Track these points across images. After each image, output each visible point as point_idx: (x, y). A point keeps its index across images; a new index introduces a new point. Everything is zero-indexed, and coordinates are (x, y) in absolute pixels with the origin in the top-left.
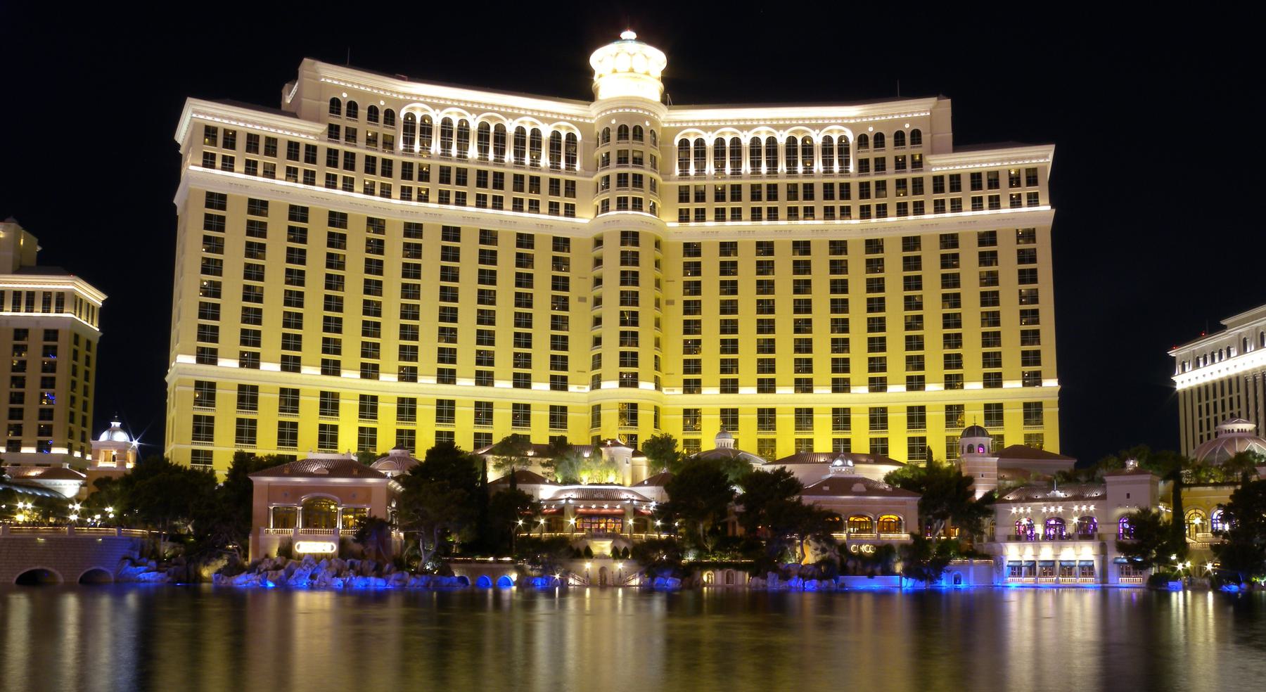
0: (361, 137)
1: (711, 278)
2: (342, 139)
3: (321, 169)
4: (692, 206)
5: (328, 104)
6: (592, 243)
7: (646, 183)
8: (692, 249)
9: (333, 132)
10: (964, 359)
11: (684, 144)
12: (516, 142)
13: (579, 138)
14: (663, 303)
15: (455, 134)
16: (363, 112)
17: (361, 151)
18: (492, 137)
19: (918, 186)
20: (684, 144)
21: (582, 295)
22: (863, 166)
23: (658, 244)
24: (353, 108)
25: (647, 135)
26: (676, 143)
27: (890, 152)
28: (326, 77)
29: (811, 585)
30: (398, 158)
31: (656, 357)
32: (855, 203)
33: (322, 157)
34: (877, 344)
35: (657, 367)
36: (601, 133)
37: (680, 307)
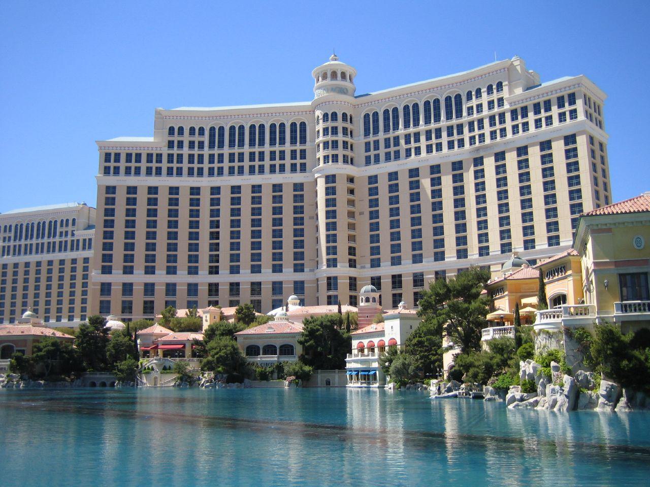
2: (176, 148)
3: (165, 165)
4: (372, 153)
5: (168, 130)
7: (340, 145)
8: (373, 179)
9: (171, 144)
10: (292, 246)
14: (356, 215)
16: (186, 132)
17: (186, 151)
20: (367, 116)
23: (351, 180)
29: (158, 386)
31: (350, 248)
33: (165, 159)
34: (193, 247)
37: (367, 215)
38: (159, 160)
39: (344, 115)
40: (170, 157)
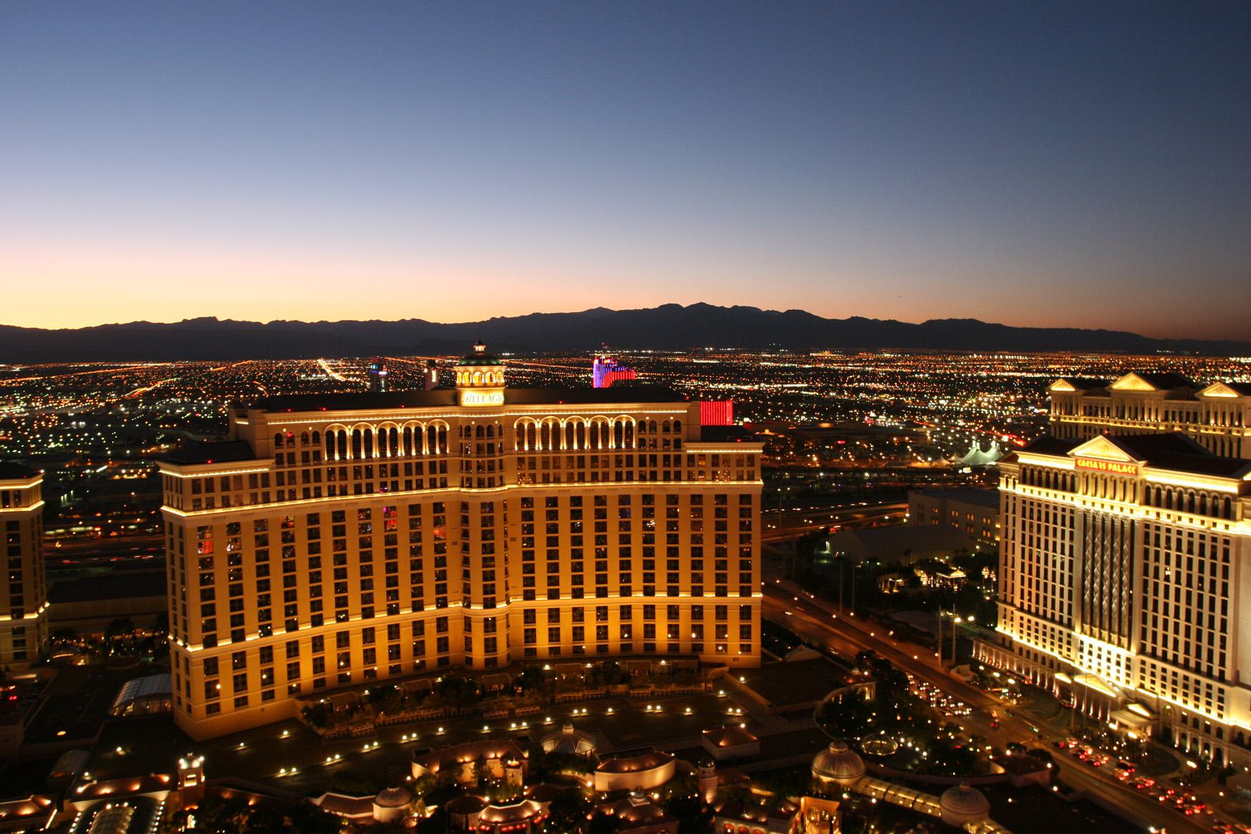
0: (299, 457)
1: (540, 523)
6: (459, 507)
11: (521, 426)
12: (405, 440)
13: (448, 429)
15: (362, 440)
16: (298, 440)
17: (299, 469)
18: (388, 439)
19: (678, 459)
20: (521, 426)
21: (454, 541)
22: (642, 443)
24: (291, 440)
25: (496, 432)
26: (515, 426)
27: (660, 436)
28: (271, 421)
30: (324, 468)
32: (636, 469)
33: (273, 481)
35: (507, 589)
36: (464, 427)
38: (266, 484)
39: (500, 428)
40: (280, 476)
